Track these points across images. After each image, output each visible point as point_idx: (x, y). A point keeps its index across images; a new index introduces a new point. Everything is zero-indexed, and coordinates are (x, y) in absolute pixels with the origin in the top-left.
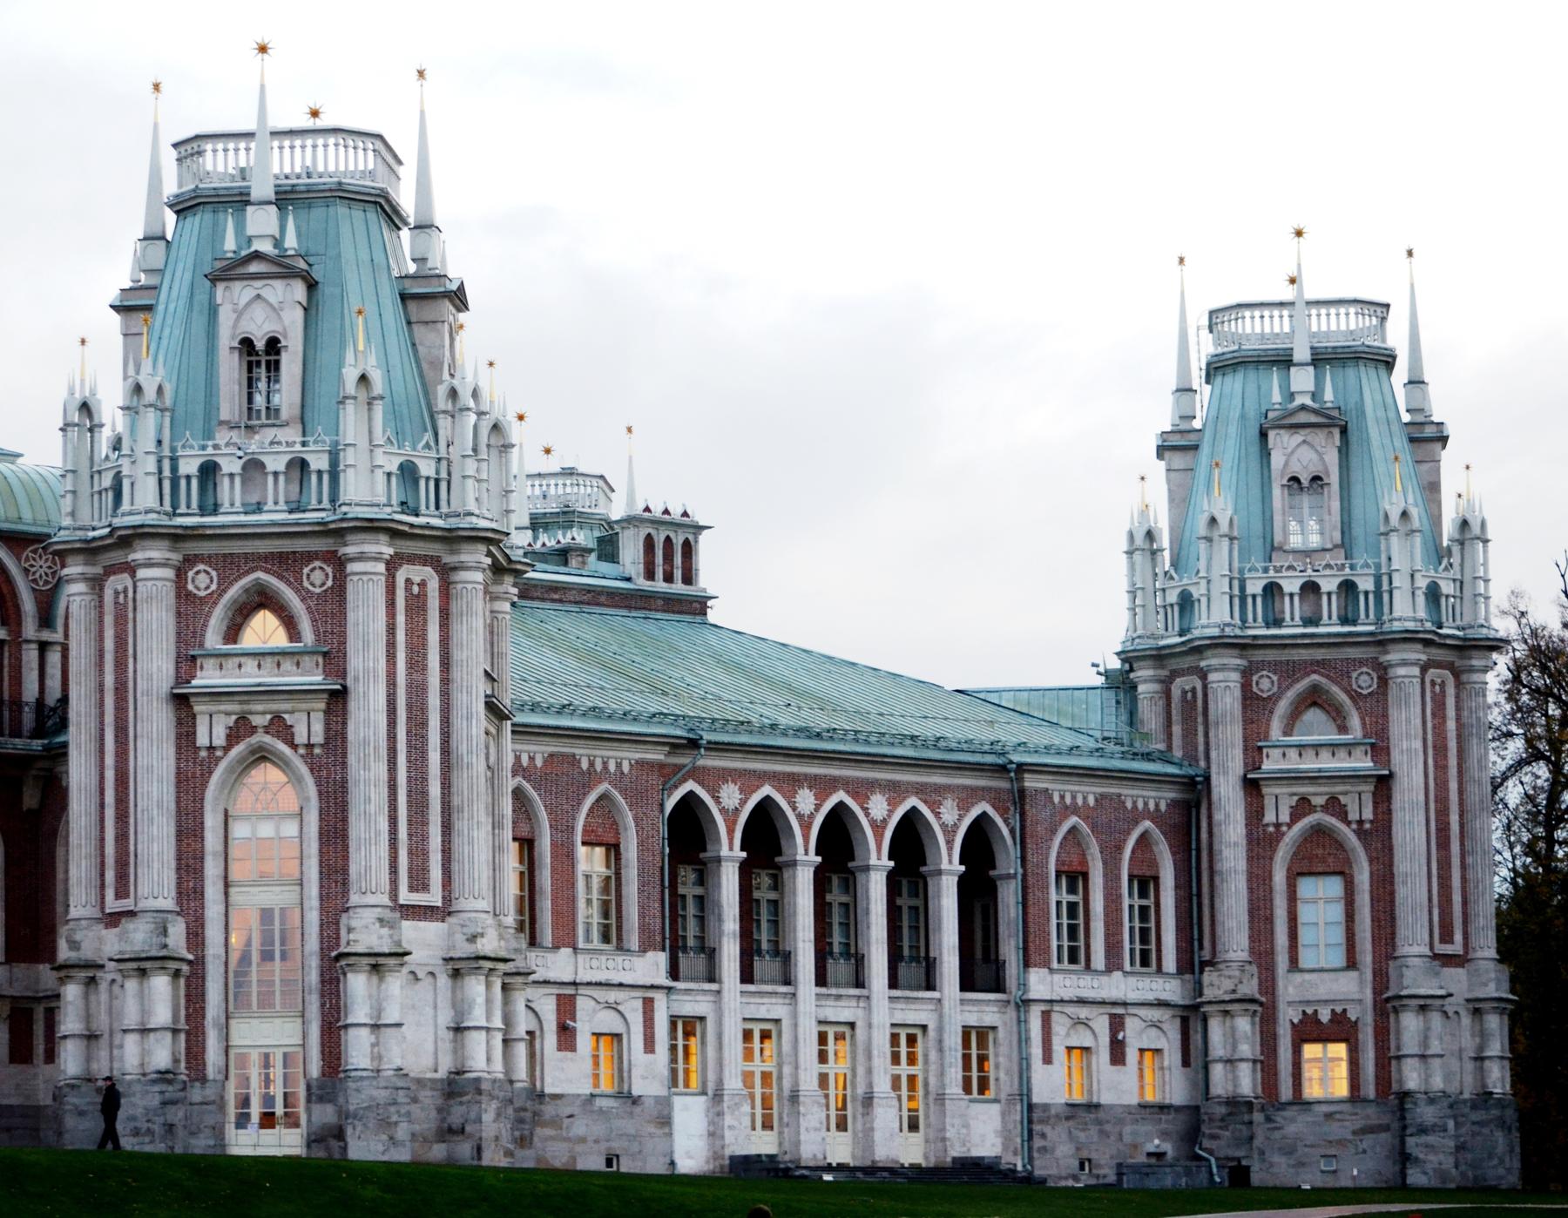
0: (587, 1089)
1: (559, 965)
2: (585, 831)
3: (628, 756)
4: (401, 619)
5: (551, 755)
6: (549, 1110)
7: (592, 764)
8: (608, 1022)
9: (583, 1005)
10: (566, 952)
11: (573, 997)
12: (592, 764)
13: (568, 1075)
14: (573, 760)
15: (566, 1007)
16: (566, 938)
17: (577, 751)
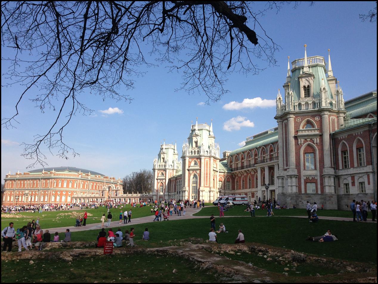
0: (357, 193)
1: (351, 171)
2: (357, 146)
3: (361, 131)
4: (284, 129)
5: (348, 135)
6: (351, 197)
7: (355, 134)
8: (361, 180)
9: (356, 178)
10: (352, 169)
11: (354, 176)
12: (355, 134)
13: (354, 190)
14: (352, 135)
15: (353, 178)
16: (353, 166)
17: (352, 133)
